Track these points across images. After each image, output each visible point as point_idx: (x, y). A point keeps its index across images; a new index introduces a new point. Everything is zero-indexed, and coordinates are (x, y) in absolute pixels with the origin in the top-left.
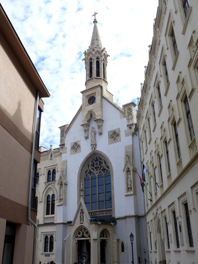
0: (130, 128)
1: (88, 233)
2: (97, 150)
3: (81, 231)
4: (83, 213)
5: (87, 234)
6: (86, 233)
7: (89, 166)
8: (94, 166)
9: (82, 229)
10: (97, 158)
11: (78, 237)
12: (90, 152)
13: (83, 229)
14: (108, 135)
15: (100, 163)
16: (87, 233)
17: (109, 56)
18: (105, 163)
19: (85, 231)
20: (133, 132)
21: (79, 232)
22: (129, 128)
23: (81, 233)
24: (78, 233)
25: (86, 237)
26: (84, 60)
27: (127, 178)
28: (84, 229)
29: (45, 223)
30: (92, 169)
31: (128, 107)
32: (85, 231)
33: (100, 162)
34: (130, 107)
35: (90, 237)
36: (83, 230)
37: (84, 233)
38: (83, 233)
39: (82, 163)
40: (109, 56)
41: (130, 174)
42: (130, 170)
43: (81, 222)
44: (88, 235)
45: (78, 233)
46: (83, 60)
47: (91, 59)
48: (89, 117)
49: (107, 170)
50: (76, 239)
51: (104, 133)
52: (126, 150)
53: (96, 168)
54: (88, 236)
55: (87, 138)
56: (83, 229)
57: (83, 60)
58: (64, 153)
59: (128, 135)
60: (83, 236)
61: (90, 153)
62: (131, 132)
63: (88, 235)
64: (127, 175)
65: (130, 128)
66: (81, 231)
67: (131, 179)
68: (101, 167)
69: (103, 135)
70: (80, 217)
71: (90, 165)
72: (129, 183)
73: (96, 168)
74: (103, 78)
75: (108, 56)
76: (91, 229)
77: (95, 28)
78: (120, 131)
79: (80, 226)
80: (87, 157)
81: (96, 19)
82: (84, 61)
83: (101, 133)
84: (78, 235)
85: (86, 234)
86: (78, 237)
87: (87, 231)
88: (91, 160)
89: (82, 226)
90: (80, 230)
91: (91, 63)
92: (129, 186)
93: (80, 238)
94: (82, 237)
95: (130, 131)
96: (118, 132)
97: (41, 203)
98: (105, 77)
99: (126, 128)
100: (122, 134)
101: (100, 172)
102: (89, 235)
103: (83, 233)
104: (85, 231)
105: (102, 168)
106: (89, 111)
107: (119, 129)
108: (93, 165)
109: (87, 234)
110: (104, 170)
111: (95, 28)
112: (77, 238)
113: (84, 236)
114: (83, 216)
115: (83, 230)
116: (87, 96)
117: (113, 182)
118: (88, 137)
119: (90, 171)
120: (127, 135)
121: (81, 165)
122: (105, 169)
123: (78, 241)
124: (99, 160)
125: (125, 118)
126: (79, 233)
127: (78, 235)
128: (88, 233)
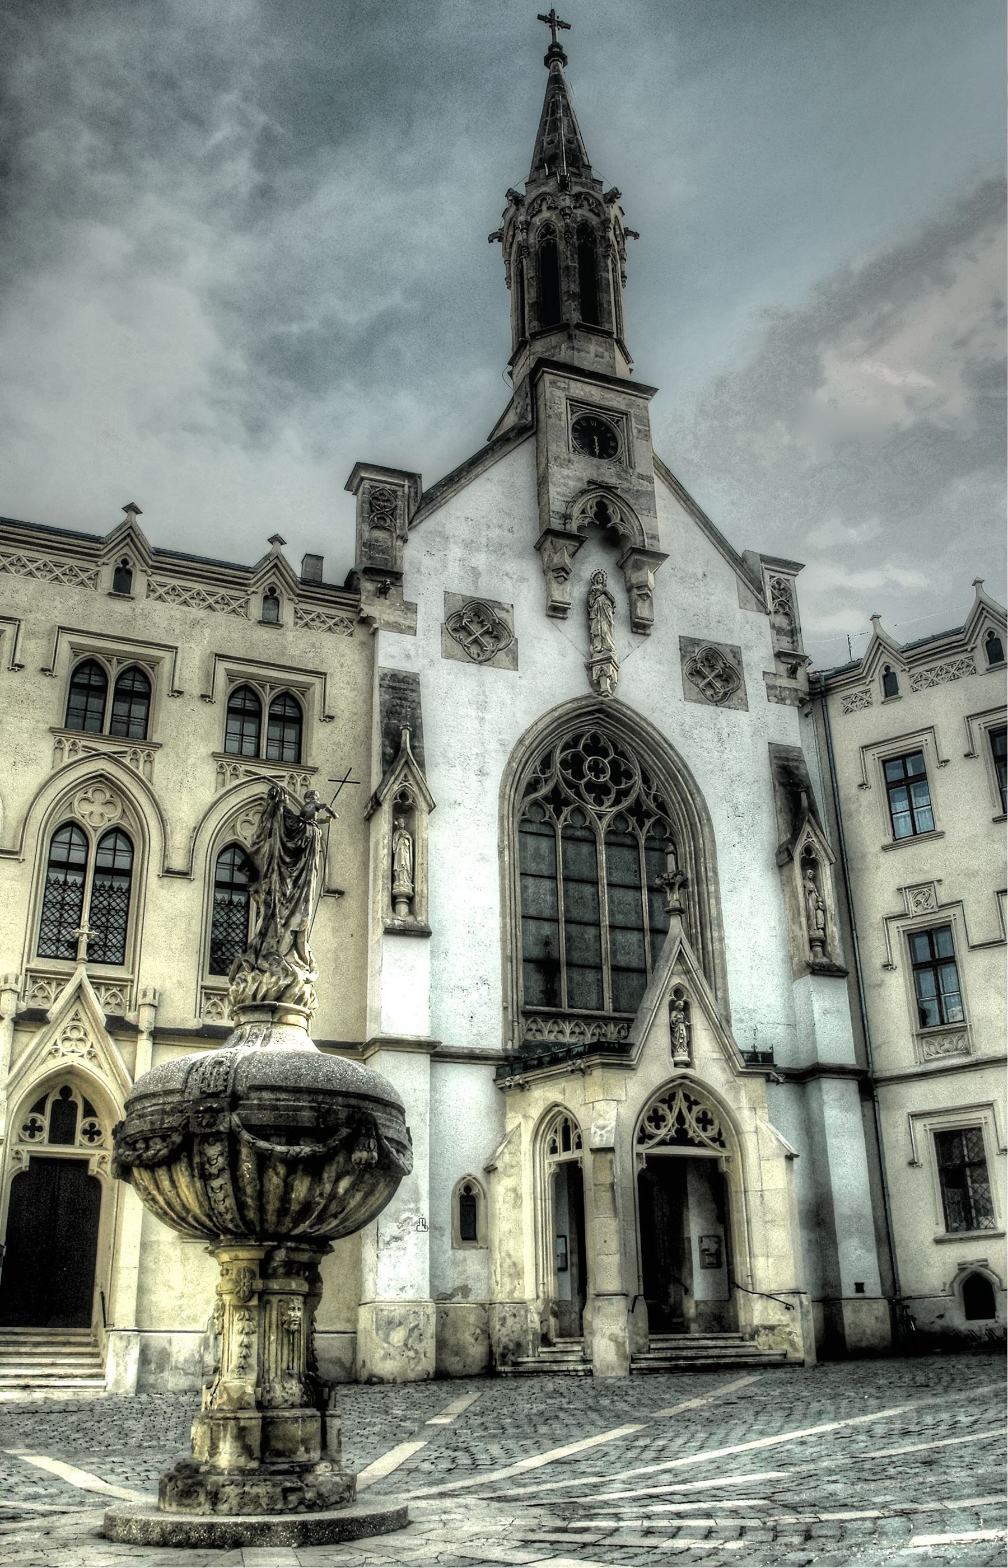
0: (793, 672)
1: (711, 1122)
2: (616, 701)
3: (671, 1108)
4: (686, 1008)
5: (705, 1129)
6: (698, 1120)
8: (579, 775)
9: (672, 1097)
10: (595, 737)
11: (651, 1137)
12: (578, 695)
13: (680, 1095)
14: (683, 657)
15: (620, 774)
16: (704, 1121)
19: (690, 1109)
20: (801, 695)
21: (655, 1111)
22: (783, 668)
23: (671, 1118)
24: (650, 1119)
25: (701, 1144)
28: (687, 1098)
29: (204, 1026)
30: (570, 785)
31: (778, 575)
32: (690, 1109)
34: (782, 576)
35: (723, 1145)
36: (679, 1103)
37: (690, 1119)
38: (680, 1119)
39: (528, 731)
42: (819, 858)
43: (682, 1056)
44: (712, 1131)
45: (650, 1119)
50: (642, 1149)
51: (657, 632)
52: (780, 763)
53: (590, 787)
54: (713, 1140)
55: (556, 611)
56: (680, 1095)
58: (397, 628)
59: (781, 700)
60: (682, 1138)
61: (576, 699)
62: (796, 690)
63: (712, 1131)
65: (793, 672)
66: (671, 1108)
68: (626, 792)
69: (650, 638)
70: (671, 1028)
71: (558, 757)
73: (590, 787)
76: (744, 1102)
78: (740, 663)
79: (673, 1081)
80: (555, 709)
83: (645, 627)
84: (650, 1129)
85: (709, 1127)
86: (651, 1137)
87: (705, 1113)
88: (566, 738)
89: (684, 1077)
90: (663, 1101)
93: (662, 1143)
94: (673, 1142)
95: (785, 682)
96: (731, 660)
97: (178, 884)
99: (772, 666)
100: (754, 684)
102: (720, 1133)
103: (680, 1119)
104: (665, 1107)
105: (626, 803)
106: (595, 485)
107: (736, 652)
108: (573, 764)
109: (705, 1129)
112: (641, 1141)
113: (691, 1134)
114: (689, 1028)
115: (679, 1103)
117: (717, 891)
120: (776, 694)
121: (521, 741)
123: (651, 1159)
124: (612, 755)
125: (763, 615)
126: (704, 1121)
127: (650, 1129)
128: (711, 1122)
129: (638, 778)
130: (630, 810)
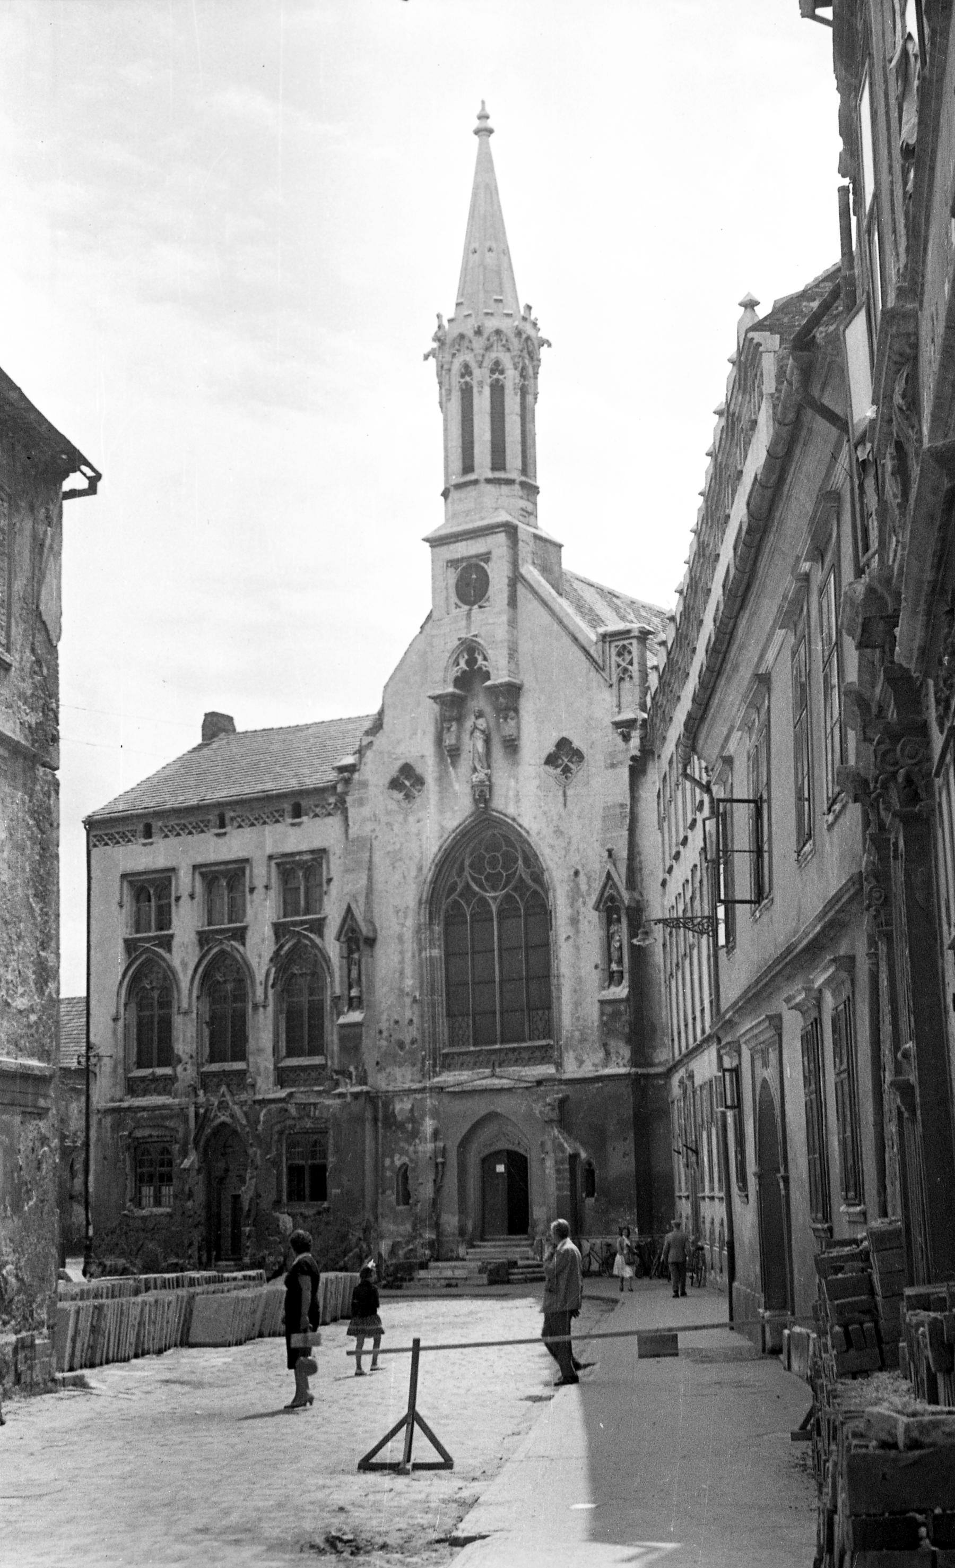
0: (626, 738)
7: (462, 869)
15: (510, 860)
17: (550, 345)
18: (526, 860)
26: (431, 358)
27: (609, 938)
30: (473, 878)
33: (505, 854)
40: (550, 345)
41: (619, 921)
46: (426, 357)
47: (467, 370)
48: (463, 664)
49: (535, 893)
57: (426, 357)
64: (609, 922)
67: (620, 941)
72: (615, 955)
74: (519, 478)
75: (544, 342)
77: (485, 163)
81: (489, 110)
82: (432, 361)
91: (467, 393)
92: (614, 967)
98: (530, 468)
100: (595, 759)
101: (508, 897)
110: (521, 886)
111: (485, 163)
116: (453, 563)
118: (458, 749)
119: (468, 886)
122: (528, 888)
129: (520, 862)
130: (515, 889)
